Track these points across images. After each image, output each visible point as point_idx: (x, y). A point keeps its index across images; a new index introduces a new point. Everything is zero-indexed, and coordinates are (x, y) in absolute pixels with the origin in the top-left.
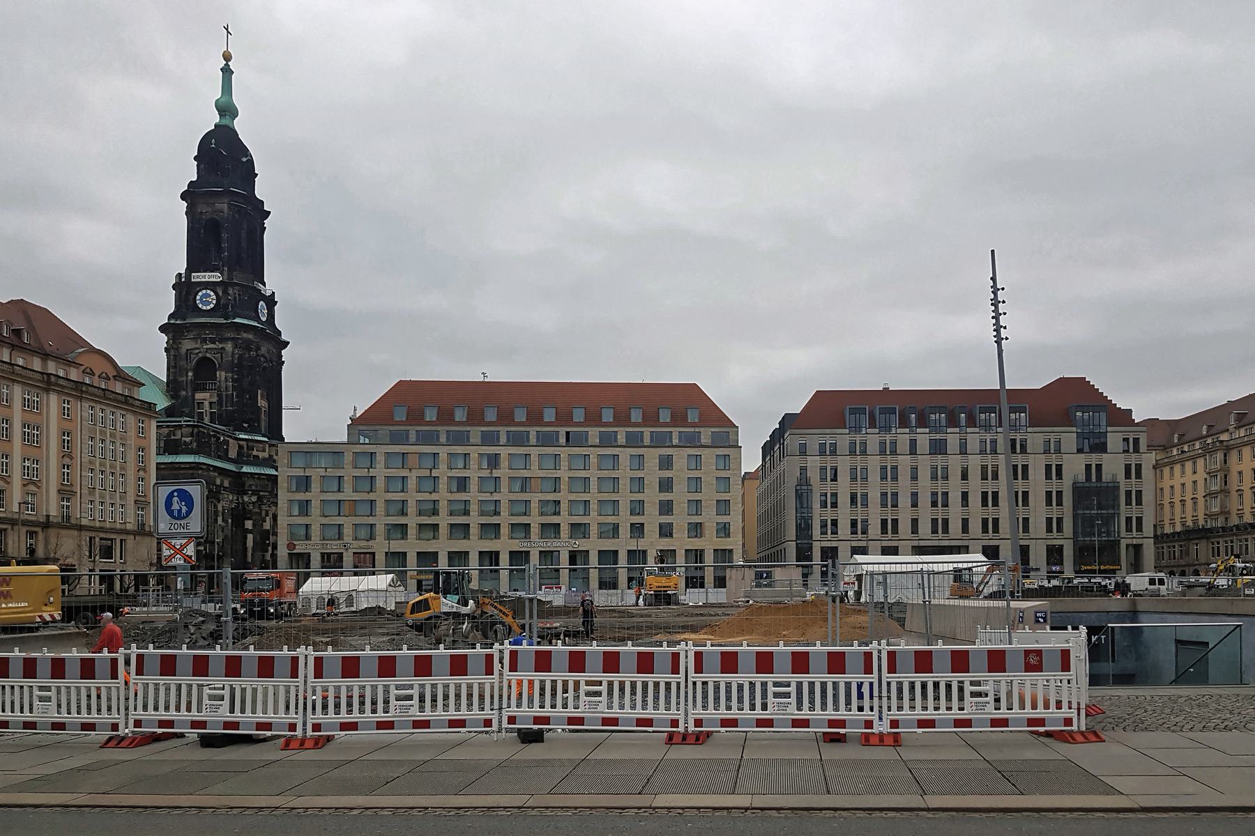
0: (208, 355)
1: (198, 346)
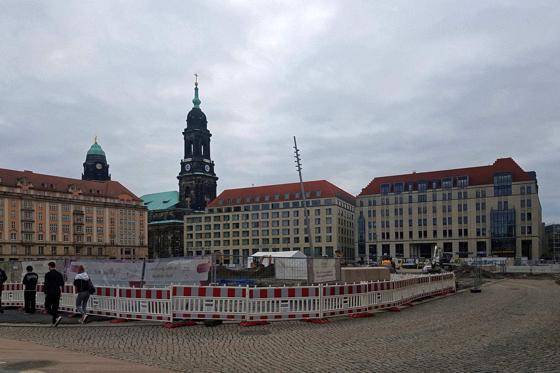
0: (188, 186)
1: (185, 183)
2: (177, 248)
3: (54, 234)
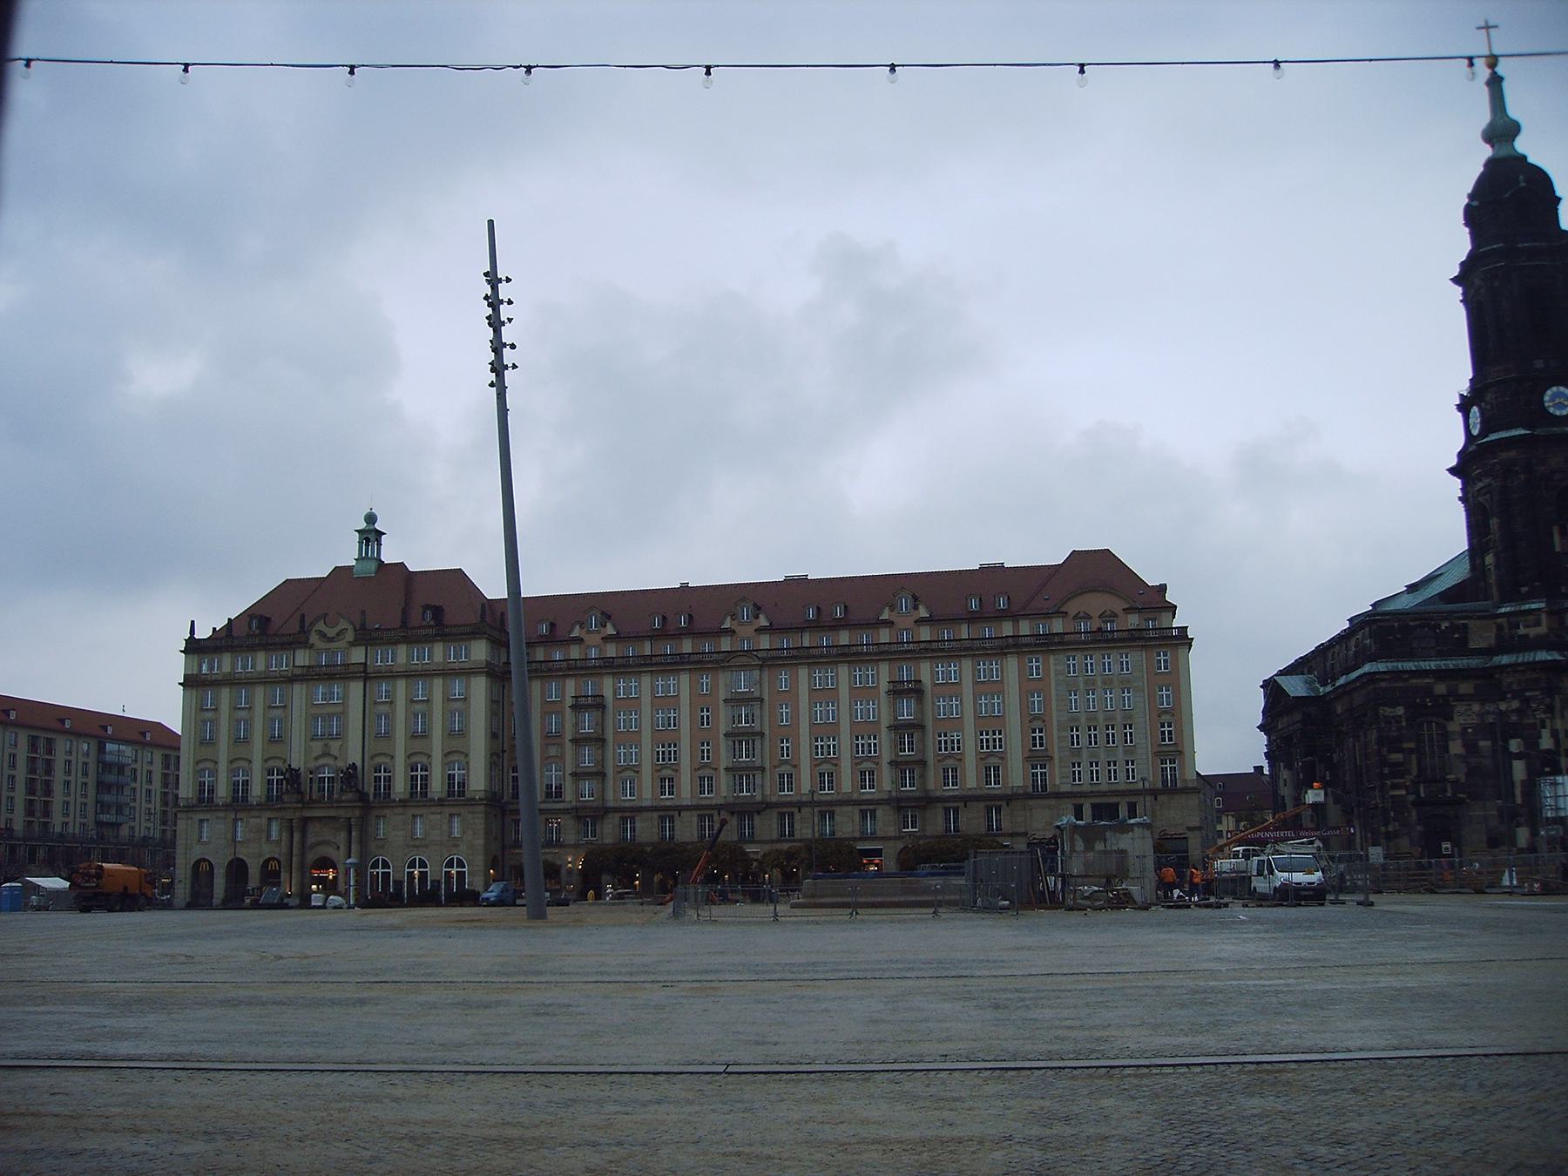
2: (1395, 787)
3: (826, 767)
